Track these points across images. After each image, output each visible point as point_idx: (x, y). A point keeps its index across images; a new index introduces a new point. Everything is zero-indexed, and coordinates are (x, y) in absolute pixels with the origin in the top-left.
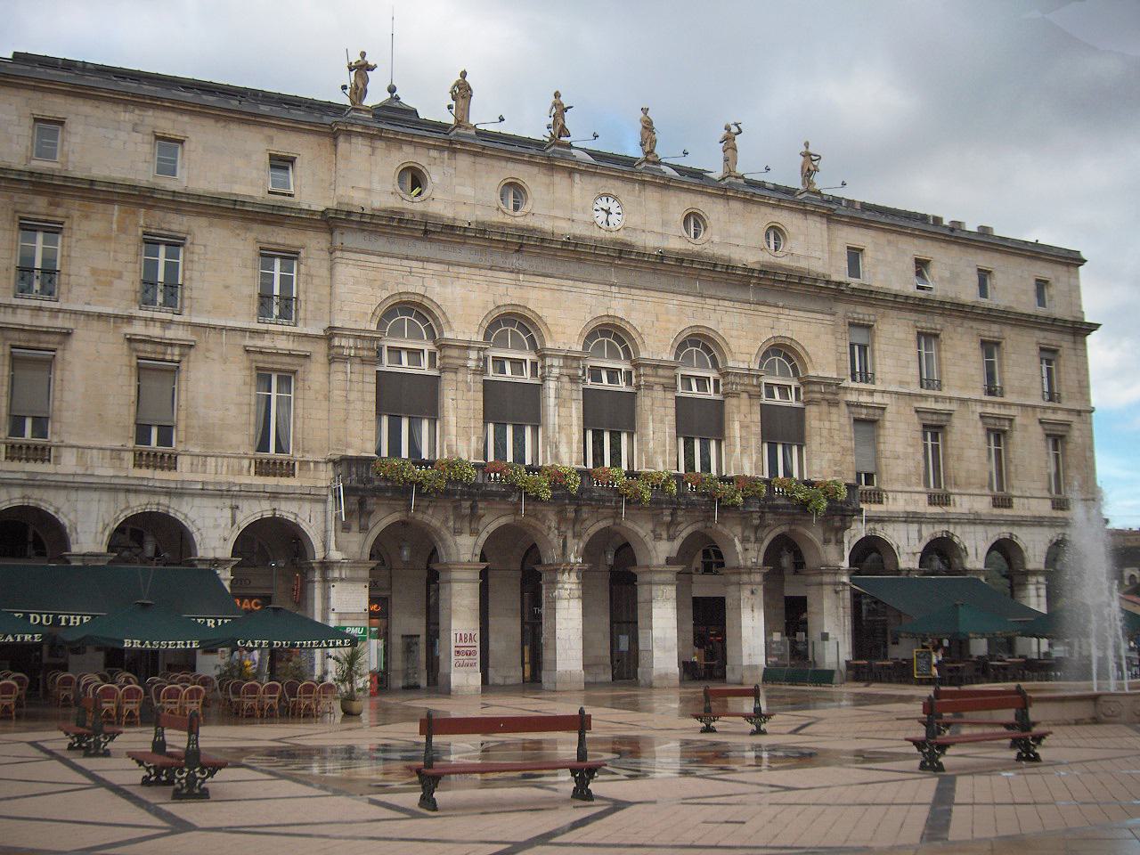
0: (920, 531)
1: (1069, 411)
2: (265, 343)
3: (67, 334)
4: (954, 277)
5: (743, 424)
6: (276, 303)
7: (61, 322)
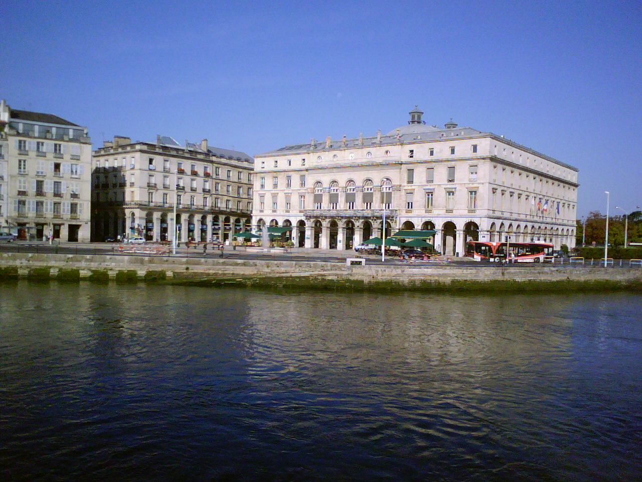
0: (421, 220)
1: (479, 183)
2: (301, 191)
3: (278, 193)
4: (441, 151)
5: (377, 198)
6: (303, 184)
7: (278, 192)
